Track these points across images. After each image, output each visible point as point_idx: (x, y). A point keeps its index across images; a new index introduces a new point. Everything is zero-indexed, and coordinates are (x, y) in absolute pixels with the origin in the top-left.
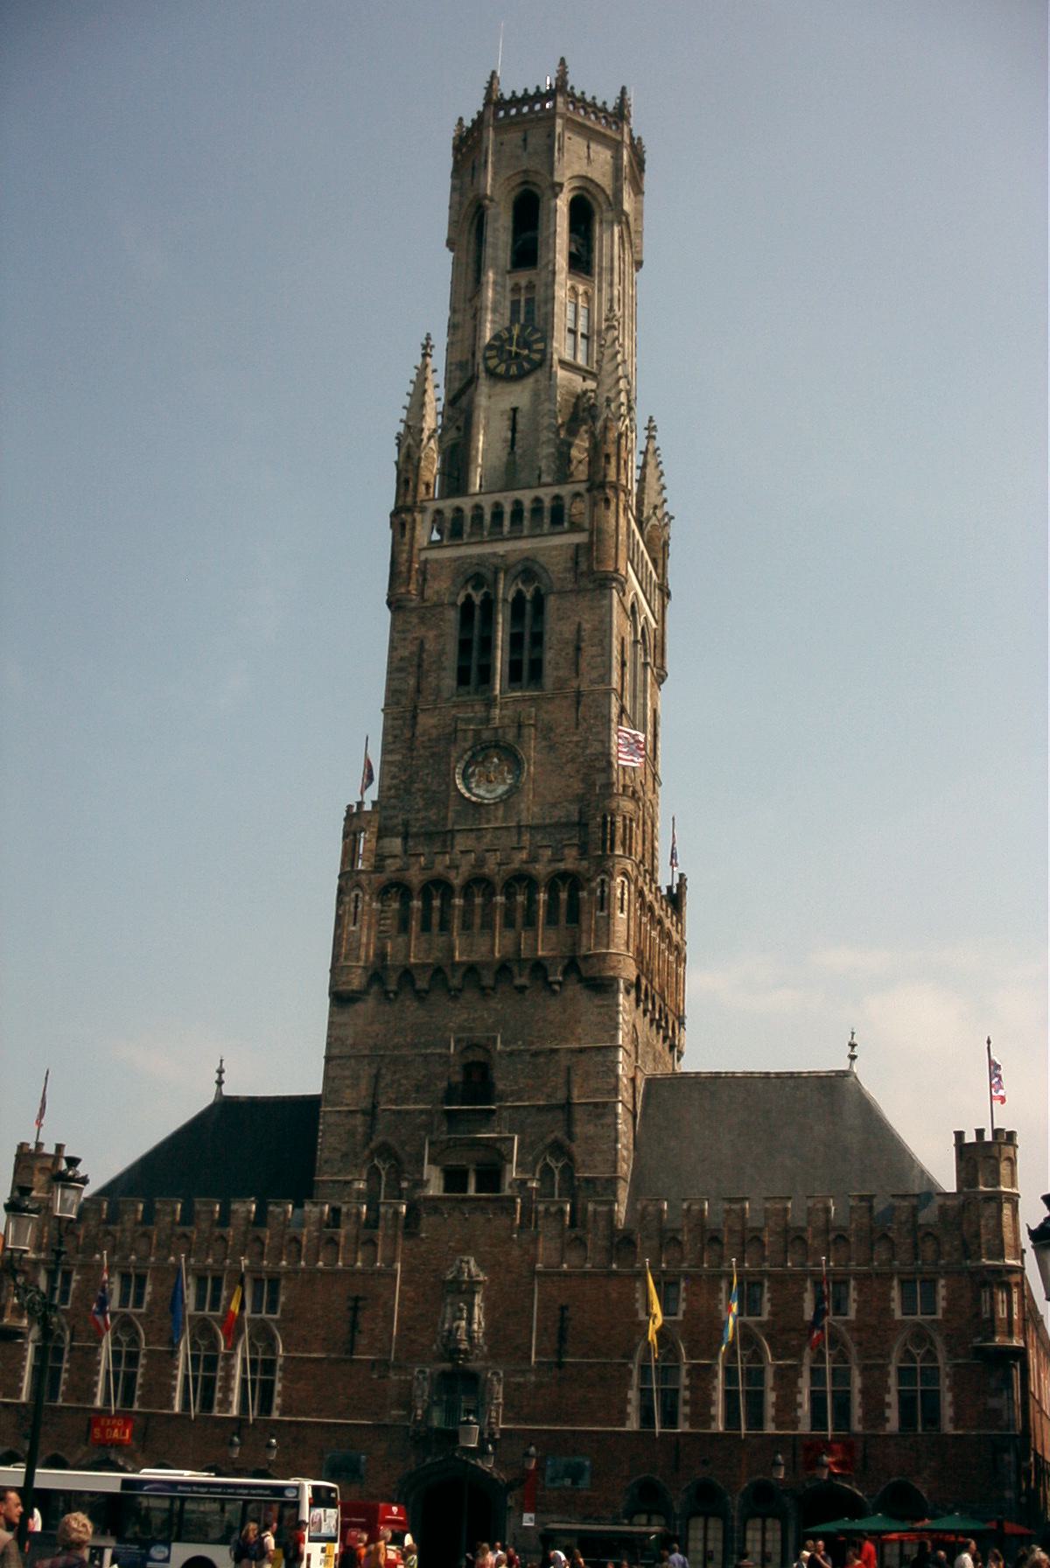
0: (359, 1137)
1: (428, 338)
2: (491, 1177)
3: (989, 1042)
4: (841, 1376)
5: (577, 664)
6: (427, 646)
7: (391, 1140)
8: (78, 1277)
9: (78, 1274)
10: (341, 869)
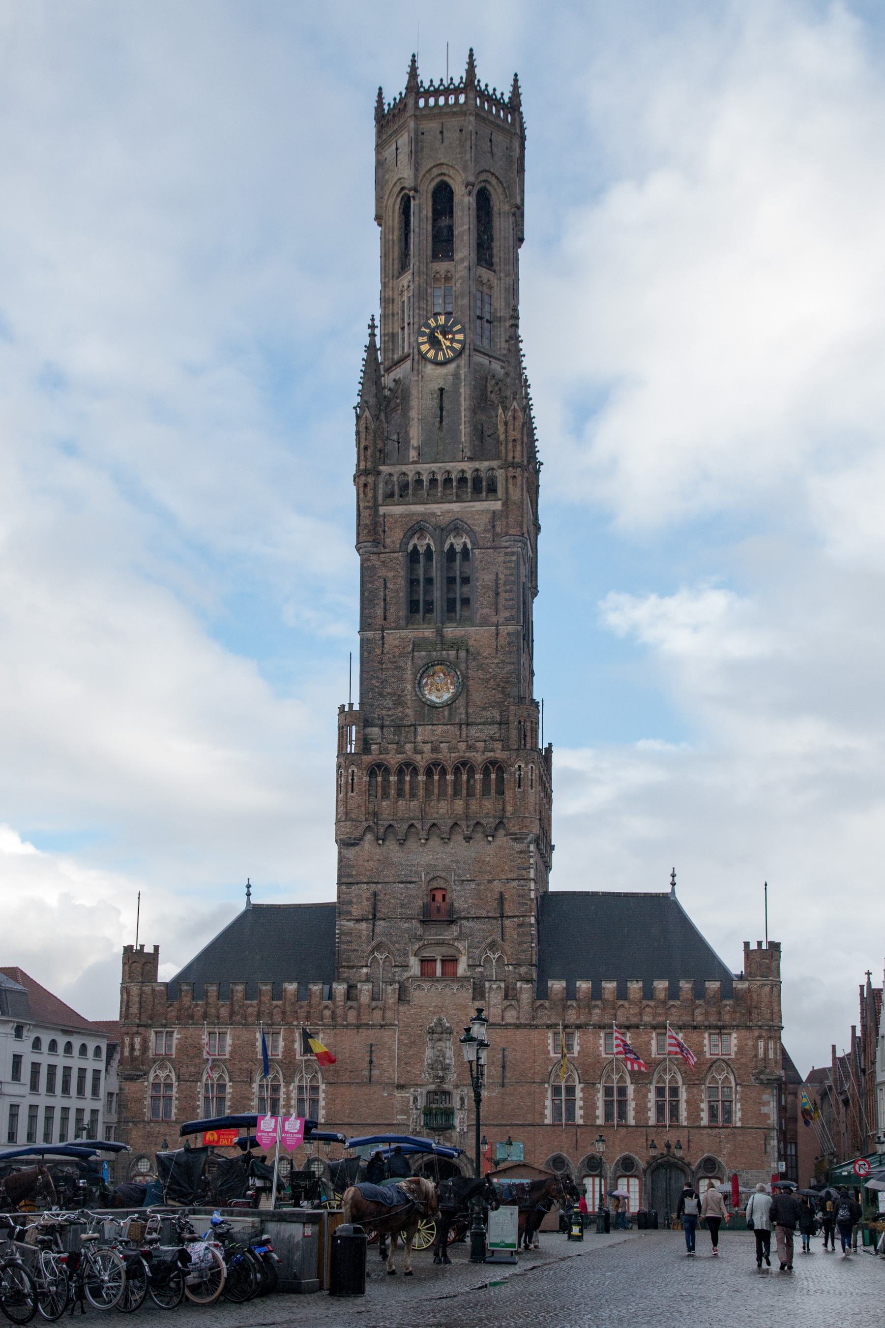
0: (364, 938)
1: (373, 320)
2: (450, 961)
3: (766, 885)
4: (674, 1091)
5: (496, 604)
6: (388, 585)
7: (384, 939)
8: (179, 1036)
9: (179, 1033)
10: (339, 751)
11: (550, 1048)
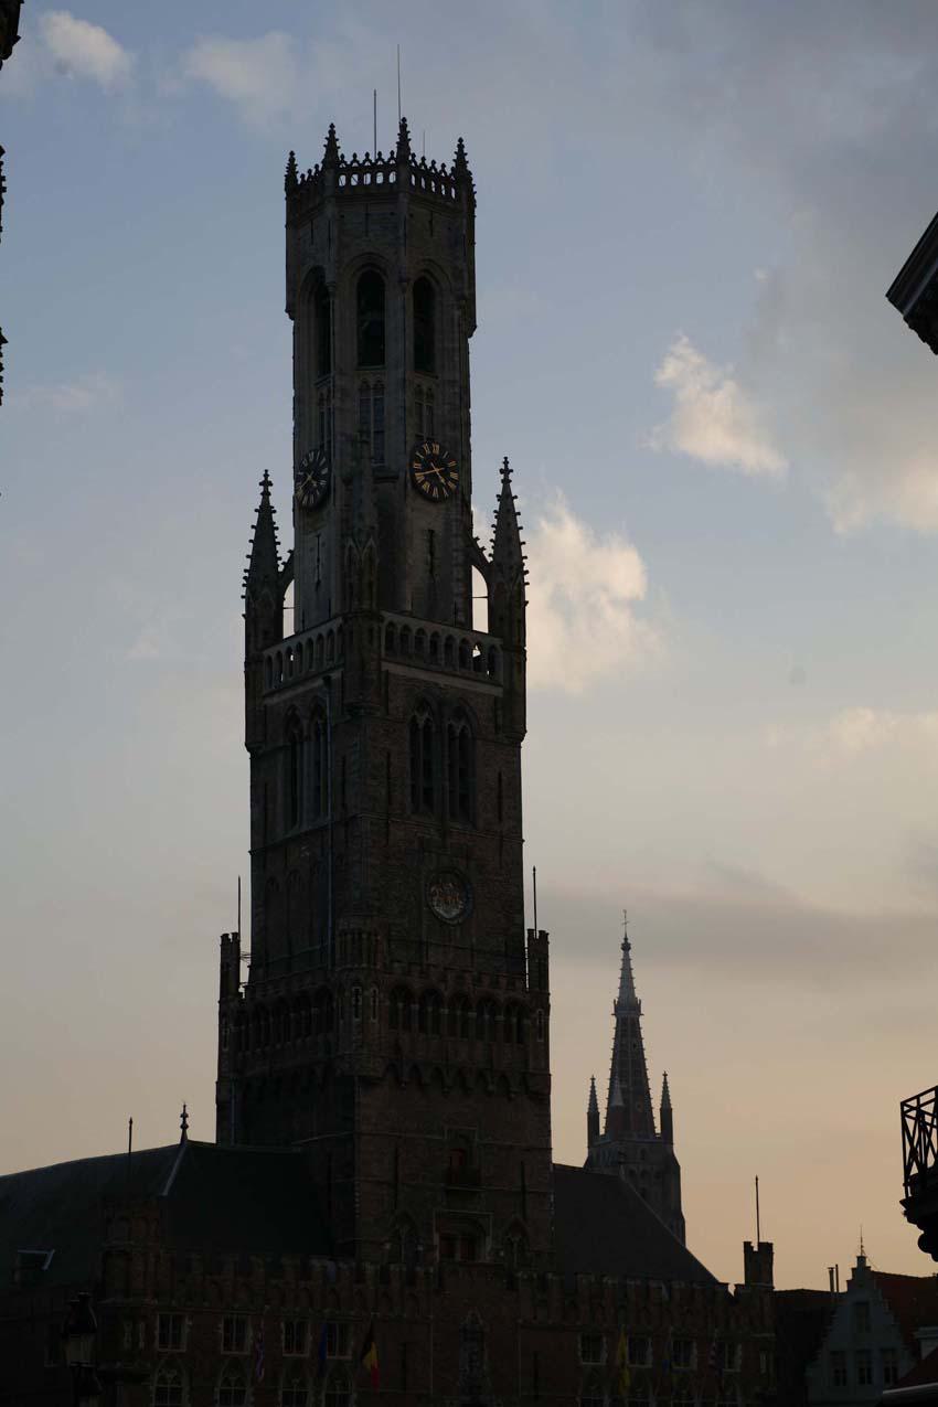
5: (500, 813)
6: (392, 760)
11: (580, 1354)
